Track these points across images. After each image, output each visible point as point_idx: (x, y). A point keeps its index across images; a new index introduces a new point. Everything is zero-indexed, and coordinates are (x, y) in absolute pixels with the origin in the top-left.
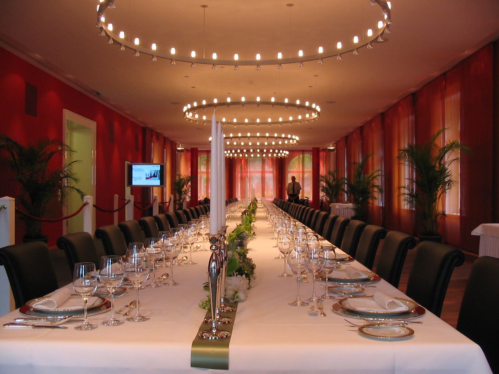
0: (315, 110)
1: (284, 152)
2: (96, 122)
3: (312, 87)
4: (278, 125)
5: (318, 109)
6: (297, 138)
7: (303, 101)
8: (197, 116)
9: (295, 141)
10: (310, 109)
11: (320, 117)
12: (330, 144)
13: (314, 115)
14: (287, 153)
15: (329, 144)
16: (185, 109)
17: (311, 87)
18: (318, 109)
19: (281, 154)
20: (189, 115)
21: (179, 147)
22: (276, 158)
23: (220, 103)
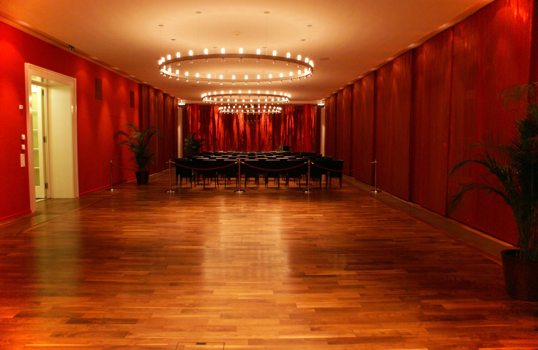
0: (308, 66)
1: (278, 108)
2: (75, 78)
3: (305, 40)
4: (268, 82)
5: (312, 63)
6: (289, 96)
7: (303, 58)
8: (178, 72)
9: (287, 99)
10: (302, 64)
11: (313, 74)
12: (320, 101)
13: (307, 72)
14: (280, 109)
15: (319, 101)
16: (160, 62)
17: (304, 41)
18: (312, 63)
19: (275, 110)
20: (167, 71)
21: (180, 103)
22: (265, 113)
23: (196, 56)
